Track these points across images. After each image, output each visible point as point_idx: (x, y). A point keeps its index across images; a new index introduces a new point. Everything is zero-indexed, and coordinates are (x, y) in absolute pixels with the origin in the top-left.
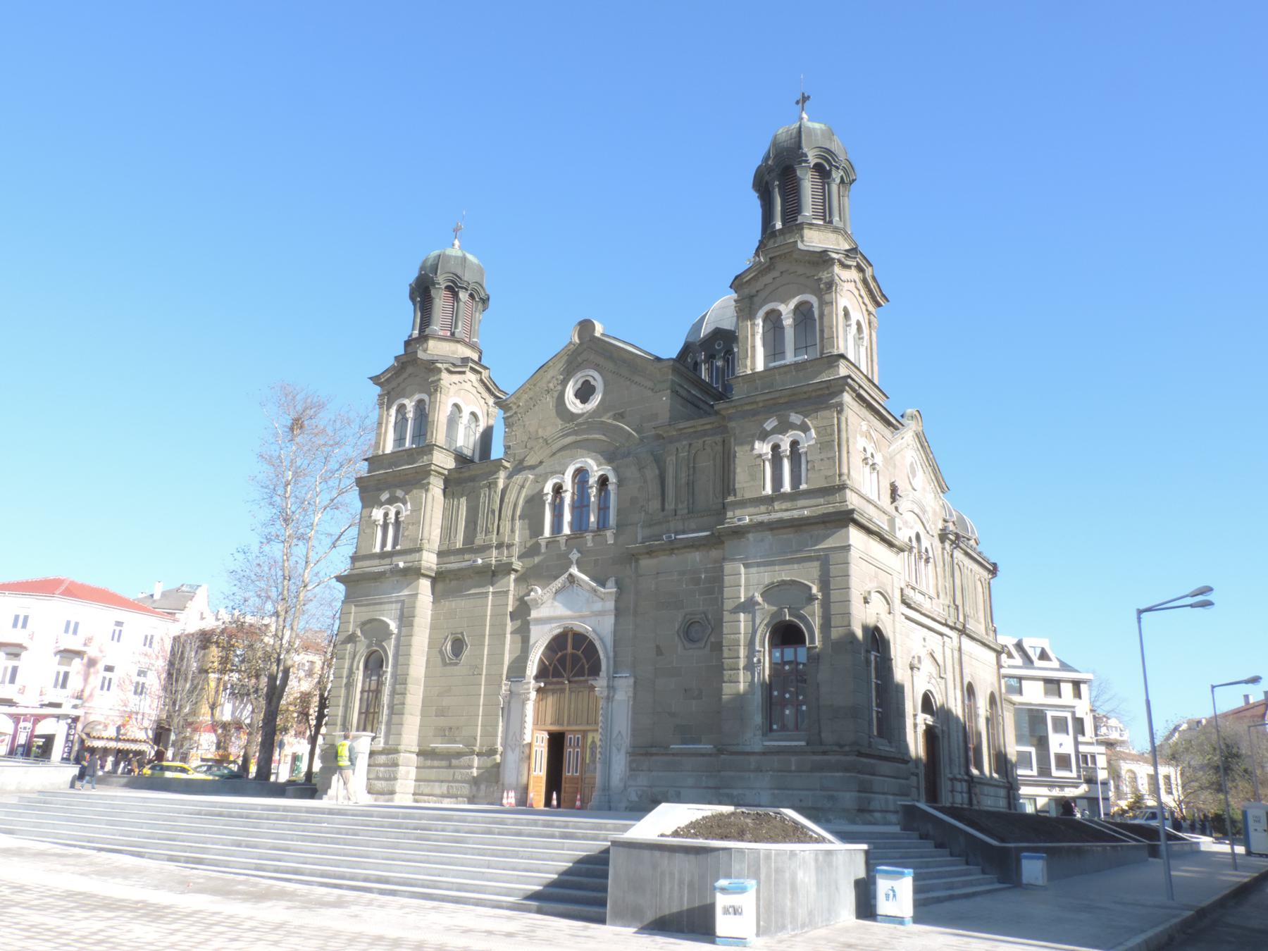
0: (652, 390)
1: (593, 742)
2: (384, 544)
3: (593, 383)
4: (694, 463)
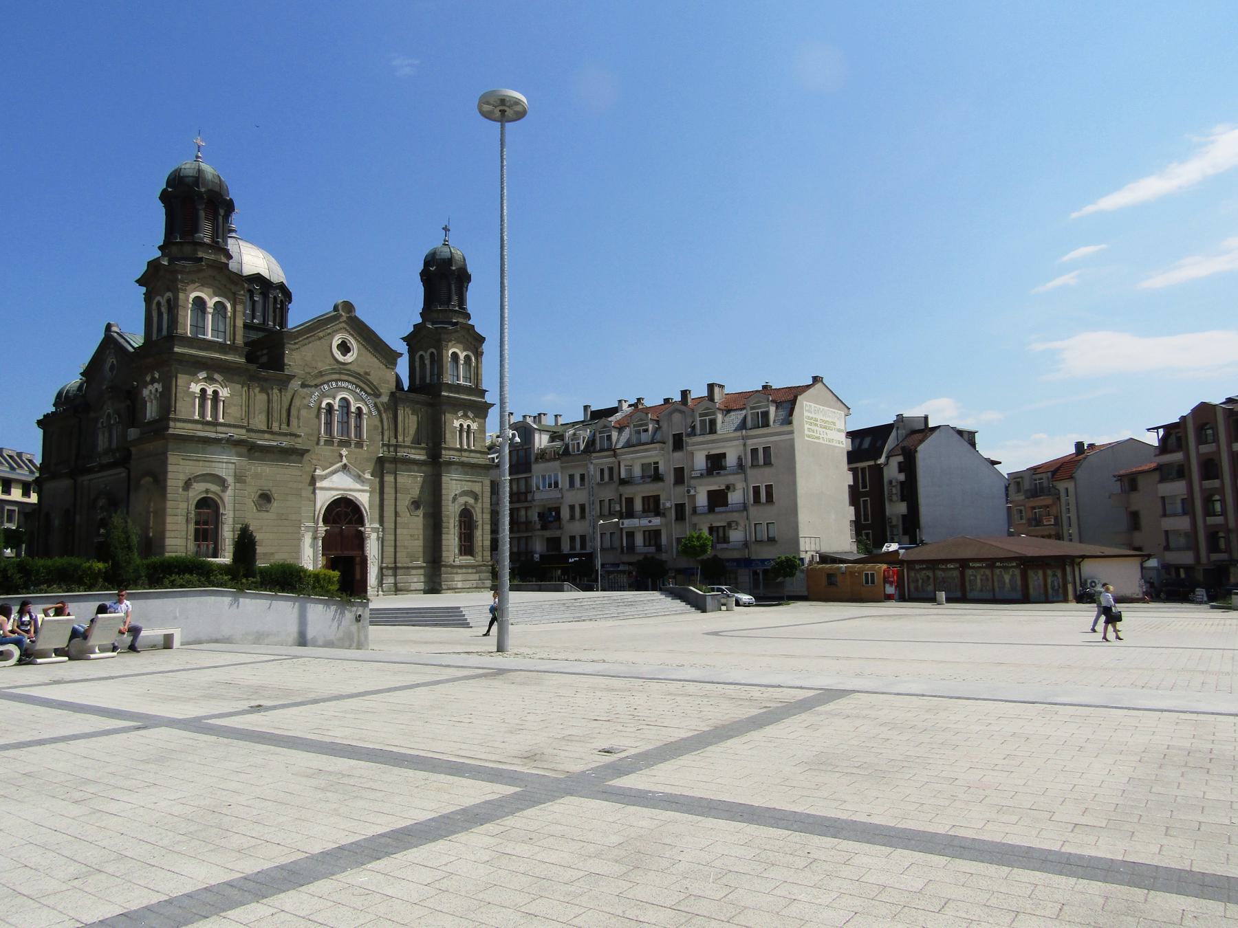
2: (202, 414)
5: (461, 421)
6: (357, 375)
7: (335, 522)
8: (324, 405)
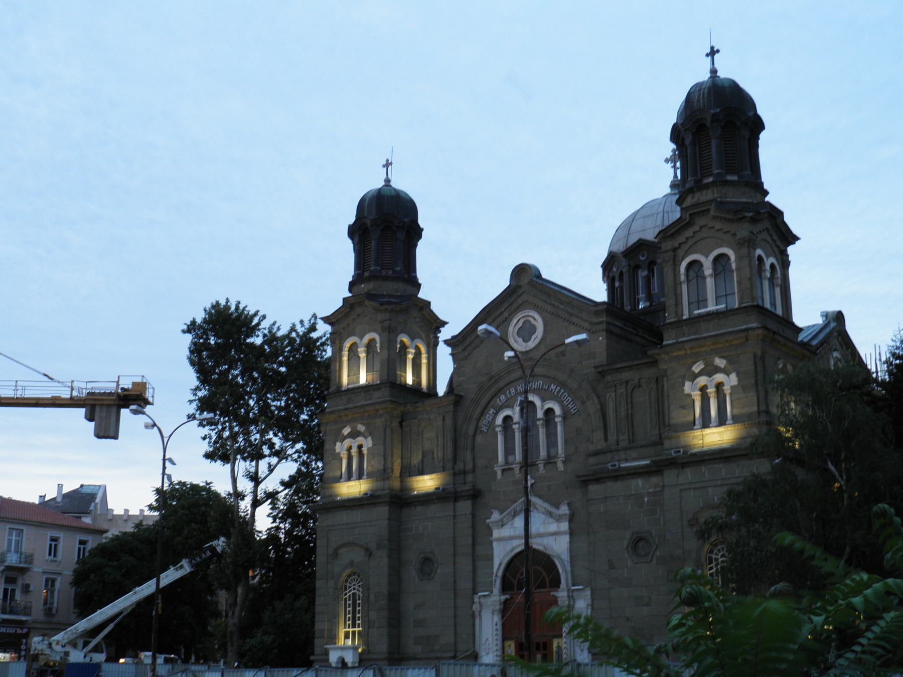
0: (589, 331)
1: (559, 647)
3: (533, 322)
4: (632, 399)
5: (702, 380)
8: (499, 420)
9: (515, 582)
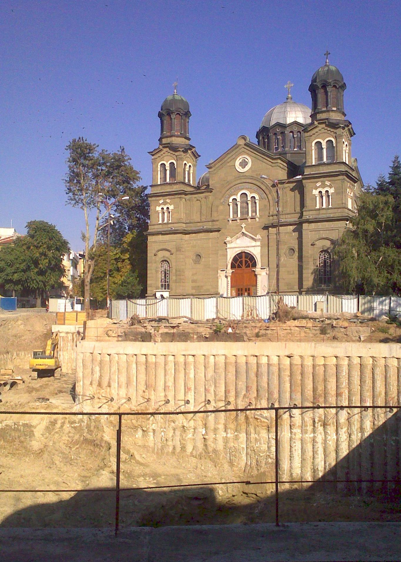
2: (163, 220)
6: (252, 178)
7: (239, 267)
8: (231, 200)
9: (236, 265)
